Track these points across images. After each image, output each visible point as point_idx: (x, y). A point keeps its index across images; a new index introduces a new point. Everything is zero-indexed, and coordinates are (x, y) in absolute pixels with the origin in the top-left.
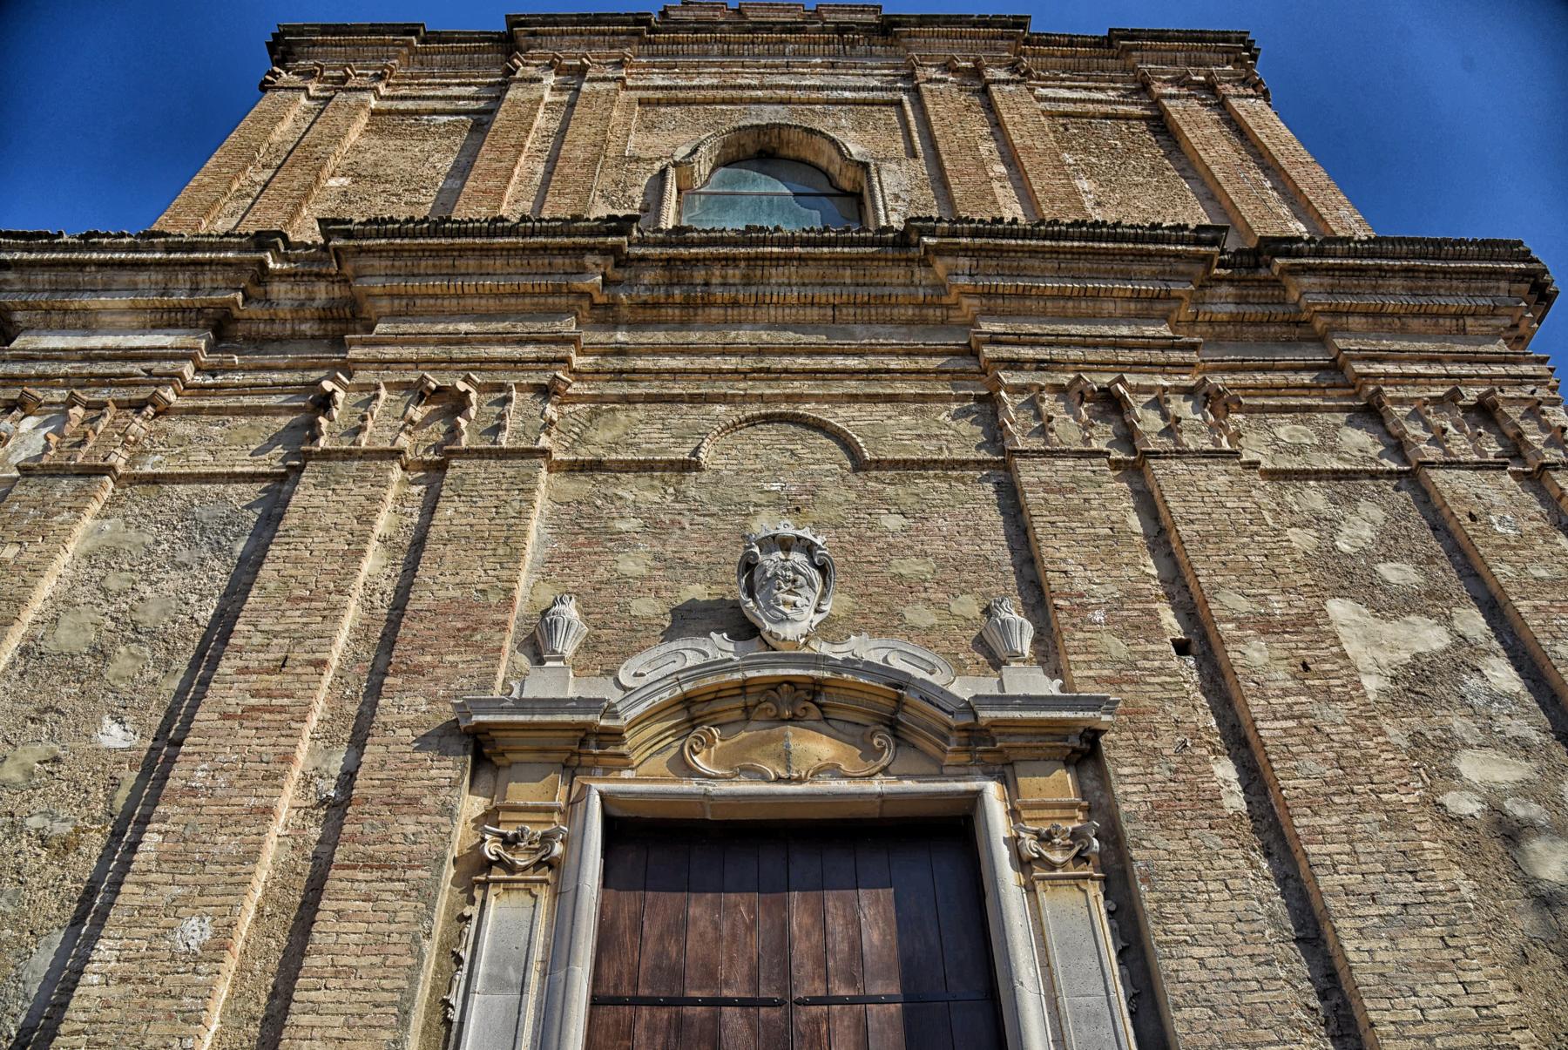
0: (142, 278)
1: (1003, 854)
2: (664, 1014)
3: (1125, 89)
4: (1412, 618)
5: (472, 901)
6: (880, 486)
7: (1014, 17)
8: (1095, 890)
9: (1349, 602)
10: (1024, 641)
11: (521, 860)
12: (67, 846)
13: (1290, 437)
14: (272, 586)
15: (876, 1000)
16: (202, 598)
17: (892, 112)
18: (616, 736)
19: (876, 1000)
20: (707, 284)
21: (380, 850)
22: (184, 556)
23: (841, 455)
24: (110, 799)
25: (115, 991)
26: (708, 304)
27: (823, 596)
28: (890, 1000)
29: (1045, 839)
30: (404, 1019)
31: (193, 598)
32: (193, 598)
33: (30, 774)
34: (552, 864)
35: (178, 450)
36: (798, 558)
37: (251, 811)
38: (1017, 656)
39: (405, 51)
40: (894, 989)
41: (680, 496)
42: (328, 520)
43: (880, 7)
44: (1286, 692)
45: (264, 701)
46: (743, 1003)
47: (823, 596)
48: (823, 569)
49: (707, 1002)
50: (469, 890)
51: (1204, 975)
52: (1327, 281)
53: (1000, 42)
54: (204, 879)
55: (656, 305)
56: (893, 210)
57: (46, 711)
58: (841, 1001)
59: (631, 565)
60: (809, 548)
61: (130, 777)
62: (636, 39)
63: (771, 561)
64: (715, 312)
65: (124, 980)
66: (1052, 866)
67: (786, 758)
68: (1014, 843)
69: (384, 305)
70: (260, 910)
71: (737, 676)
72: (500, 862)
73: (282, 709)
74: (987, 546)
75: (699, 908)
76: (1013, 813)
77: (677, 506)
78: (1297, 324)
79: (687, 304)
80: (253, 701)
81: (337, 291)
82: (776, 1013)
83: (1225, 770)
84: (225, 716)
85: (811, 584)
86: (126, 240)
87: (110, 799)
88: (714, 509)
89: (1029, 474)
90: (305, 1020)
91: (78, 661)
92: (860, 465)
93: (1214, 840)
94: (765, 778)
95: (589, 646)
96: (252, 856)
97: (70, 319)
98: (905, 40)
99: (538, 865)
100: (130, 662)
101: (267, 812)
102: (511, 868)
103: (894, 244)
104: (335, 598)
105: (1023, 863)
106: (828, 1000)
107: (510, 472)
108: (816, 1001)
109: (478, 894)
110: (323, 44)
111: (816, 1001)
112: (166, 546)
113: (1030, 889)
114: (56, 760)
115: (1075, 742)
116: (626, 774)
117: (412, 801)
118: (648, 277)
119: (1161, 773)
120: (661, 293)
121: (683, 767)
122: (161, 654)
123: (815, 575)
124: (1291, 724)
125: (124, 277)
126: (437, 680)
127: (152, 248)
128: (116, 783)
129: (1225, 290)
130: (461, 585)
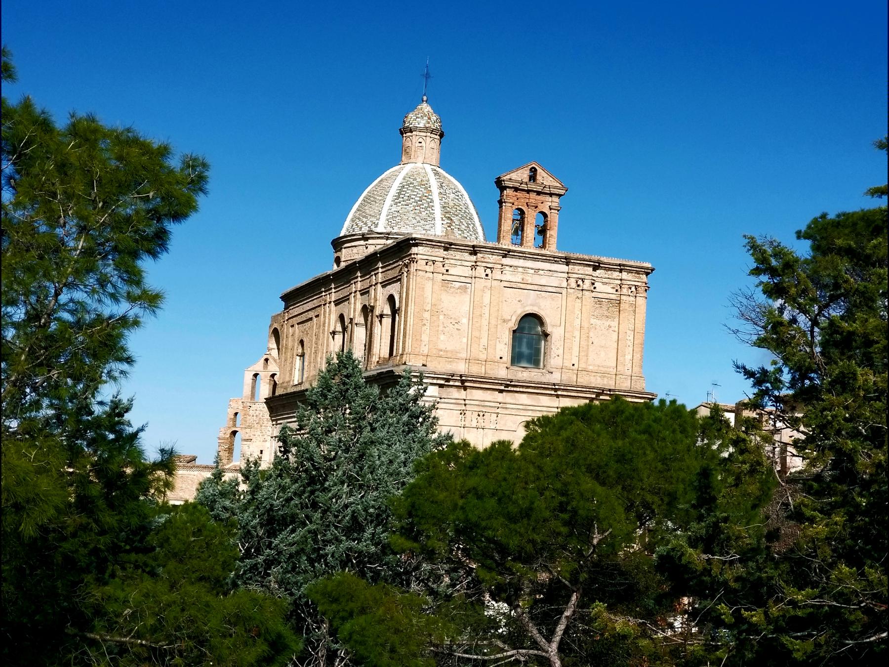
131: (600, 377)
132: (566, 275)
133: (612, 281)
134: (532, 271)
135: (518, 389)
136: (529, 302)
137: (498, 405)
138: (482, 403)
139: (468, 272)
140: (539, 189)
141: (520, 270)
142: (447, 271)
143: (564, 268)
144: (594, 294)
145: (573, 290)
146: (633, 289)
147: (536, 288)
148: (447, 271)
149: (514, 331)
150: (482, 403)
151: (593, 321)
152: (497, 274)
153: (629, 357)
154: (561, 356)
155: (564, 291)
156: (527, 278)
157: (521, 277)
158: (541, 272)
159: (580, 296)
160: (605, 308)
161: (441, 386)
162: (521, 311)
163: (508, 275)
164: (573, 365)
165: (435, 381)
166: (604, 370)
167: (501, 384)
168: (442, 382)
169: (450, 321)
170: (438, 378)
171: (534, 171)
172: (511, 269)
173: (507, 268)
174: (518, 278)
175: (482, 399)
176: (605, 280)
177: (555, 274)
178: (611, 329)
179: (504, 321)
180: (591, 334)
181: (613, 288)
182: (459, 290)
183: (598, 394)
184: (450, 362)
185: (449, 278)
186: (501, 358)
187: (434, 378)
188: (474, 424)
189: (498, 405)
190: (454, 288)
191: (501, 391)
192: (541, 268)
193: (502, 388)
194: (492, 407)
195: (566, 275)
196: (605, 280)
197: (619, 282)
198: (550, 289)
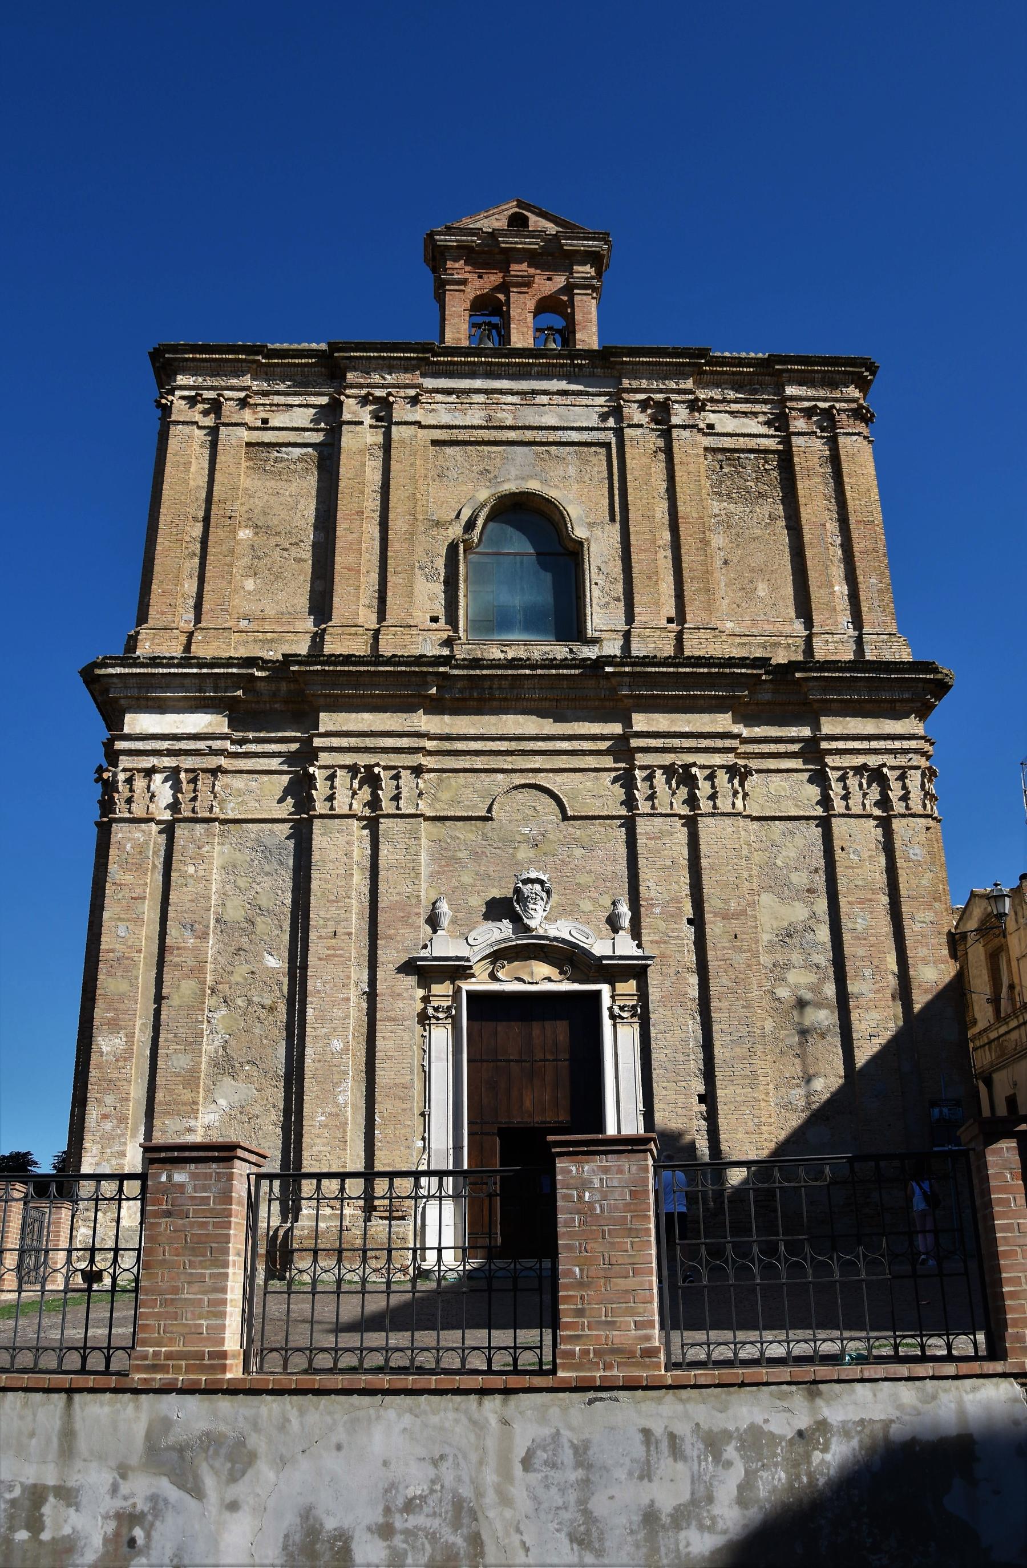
0: (187, 681)
1: (606, 1014)
2: (491, 1065)
3: (772, 414)
4: (796, 903)
5: (425, 1030)
6: (574, 830)
7: (699, 349)
8: (637, 1026)
9: (771, 895)
10: (626, 923)
11: (441, 1015)
12: (272, 1009)
13: (776, 791)
14: (319, 894)
15: (560, 1060)
16: (283, 892)
17: (603, 451)
18: (470, 968)
19: (560, 1060)
20: (491, 688)
21: (392, 1014)
22: (267, 868)
23: (557, 810)
24: (281, 990)
25: (317, 1065)
26: (492, 699)
27: (547, 903)
28: (565, 1060)
29: (622, 1008)
30: (412, 1072)
31: (280, 892)
32: (280, 892)
33: (246, 979)
34: (452, 1017)
35: (240, 799)
36: (538, 887)
37: (342, 999)
38: (621, 928)
39: (254, 366)
40: (567, 1057)
41: (485, 837)
42: (333, 856)
43: (608, 234)
44: (724, 948)
45: (333, 952)
46: (517, 1061)
47: (547, 903)
48: (548, 892)
49: (505, 1061)
50: (423, 1026)
51: (666, 1059)
52: (823, 683)
53: (687, 369)
54: (334, 1026)
55: (464, 699)
56: (596, 584)
57: (239, 949)
58: (549, 1060)
59: (467, 879)
60: (541, 882)
61: (286, 980)
62: (423, 363)
63: (527, 889)
64: (495, 704)
65: (319, 1061)
66: (623, 1018)
67: (532, 974)
68: (610, 1009)
69: (322, 701)
70: (353, 1034)
71: (514, 943)
72: (434, 1017)
73: (341, 956)
74: (618, 867)
75: (501, 1027)
76: (613, 997)
77: (484, 843)
78: (804, 704)
79: (480, 700)
80: (329, 952)
81: (292, 686)
82: (527, 1064)
83: (694, 980)
84: (320, 959)
85: (542, 899)
86: (176, 661)
87: (281, 990)
88: (500, 845)
89: (642, 826)
90: (381, 1073)
91: (242, 926)
92: (565, 818)
93: (680, 1011)
94: (524, 982)
95: (454, 921)
96: (347, 1017)
97: (150, 703)
98: (618, 367)
99: (446, 1018)
100: (264, 926)
101: (348, 999)
102: (438, 1019)
103: (589, 667)
104: (347, 900)
105: (613, 1017)
106: (545, 1060)
107: (409, 827)
108: (541, 1061)
109: (427, 1028)
110: (193, 359)
111: (541, 1061)
112: (256, 862)
113: (614, 1026)
114: (253, 972)
115: (638, 970)
116: (473, 980)
117: (399, 995)
118: (459, 685)
119: (668, 984)
120: (467, 695)
121: (493, 977)
122: (276, 922)
123: (544, 895)
124: (722, 963)
125: (177, 681)
126: (398, 942)
127: (191, 666)
128: (280, 983)
129: (768, 686)
130: (399, 894)
133: (757, 408)
136: (514, 472)
138: (370, 742)
140: (532, 244)
141: (481, 398)
145: (639, 431)
147: (529, 435)
148: (265, 421)
150: (370, 742)
151: (716, 506)
157: (483, 414)
169: (273, 541)
172: (453, 398)
173: (439, 397)
174: (476, 417)
176: (735, 407)
179: (437, 524)
182: (300, 466)
184: (272, 641)
185: (268, 437)
190: (282, 460)
196: (735, 407)
198: (575, 436)
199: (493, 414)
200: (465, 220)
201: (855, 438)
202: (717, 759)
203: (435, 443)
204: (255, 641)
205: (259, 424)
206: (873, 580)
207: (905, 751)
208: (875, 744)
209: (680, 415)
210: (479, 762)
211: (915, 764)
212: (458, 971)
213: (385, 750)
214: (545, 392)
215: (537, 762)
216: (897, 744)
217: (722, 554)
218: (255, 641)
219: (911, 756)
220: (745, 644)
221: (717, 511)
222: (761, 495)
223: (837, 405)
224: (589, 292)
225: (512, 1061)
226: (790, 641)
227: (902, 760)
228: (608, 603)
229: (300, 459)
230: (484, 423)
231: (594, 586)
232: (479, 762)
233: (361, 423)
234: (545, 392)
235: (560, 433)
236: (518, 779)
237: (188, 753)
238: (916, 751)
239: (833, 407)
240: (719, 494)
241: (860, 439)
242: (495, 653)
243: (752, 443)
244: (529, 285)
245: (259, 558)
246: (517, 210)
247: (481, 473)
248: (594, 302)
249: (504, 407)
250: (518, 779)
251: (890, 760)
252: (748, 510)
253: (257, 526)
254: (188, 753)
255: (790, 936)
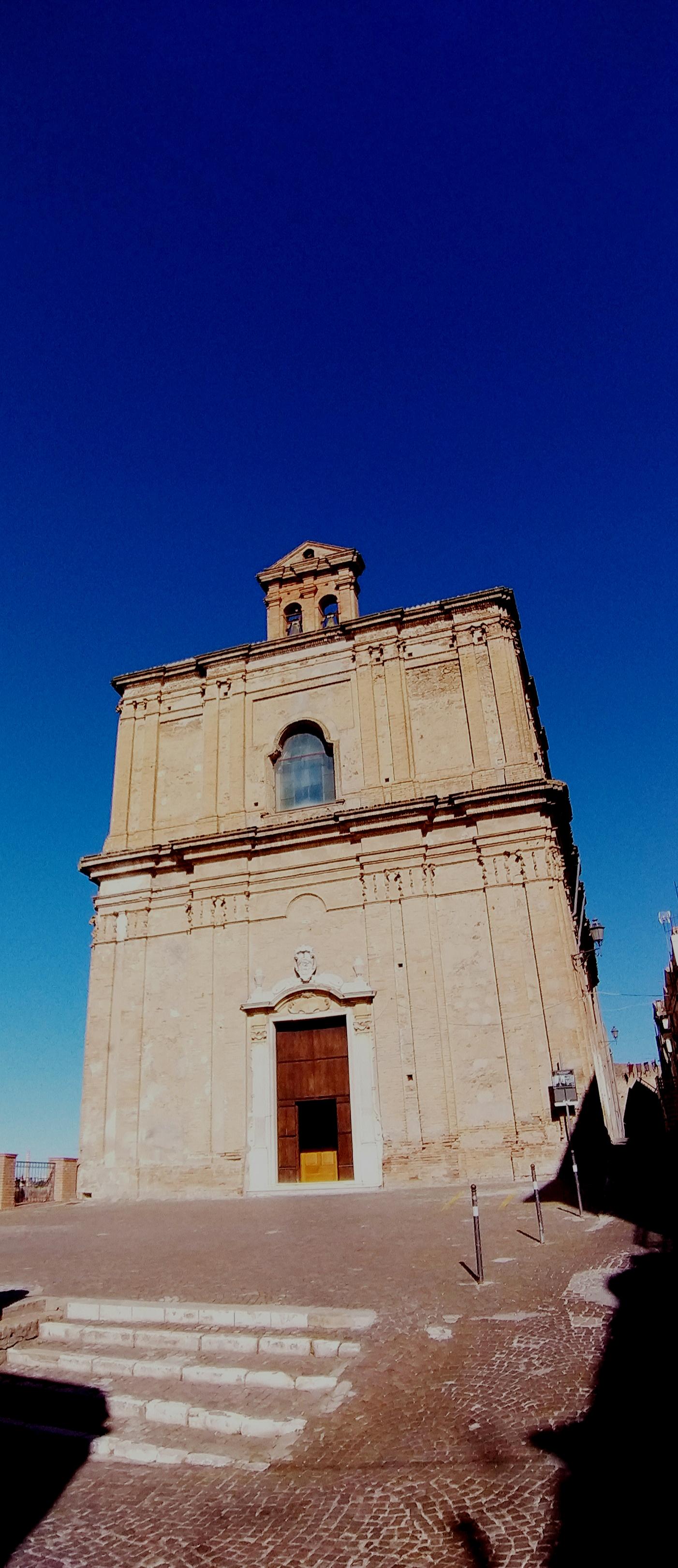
131: (443, 786)
132: (350, 653)
133: (438, 635)
134: (298, 665)
135: (279, 844)
137: (246, 878)
139: (198, 699)
142: (169, 708)
143: (344, 644)
144: (409, 664)
146: (478, 634)
148: (169, 708)
149: (274, 758)
151: (414, 703)
152: (238, 686)
153: (494, 739)
154: (361, 773)
155: (352, 675)
156: (289, 676)
157: (280, 678)
158: (311, 662)
159: (381, 673)
160: (435, 678)
161: (153, 872)
162: (281, 725)
163: (257, 682)
164: (387, 780)
165: (139, 866)
166: (447, 774)
167: (242, 842)
168: (151, 864)
170: (141, 860)
171: (309, 554)
174: (276, 681)
175: (216, 875)
176: (424, 639)
177: (336, 656)
178: (454, 705)
180: (415, 724)
181: (444, 644)
182: (188, 729)
183: (431, 812)
186: (256, 804)
187: (133, 861)
188: (207, 920)
189: (246, 878)
191: (250, 855)
192: (308, 656)
193: (248, 847)
194: (234, 884)
195: (350, 653)
196: (424, 639)
197: (450, 633)
199: (284, 677)
200: (279, 562)
201: (498, 640)
202: (413, 862)
203: (255, 701)
204: (165, 834)
205: (167, 710)
206: (512, 730)
207: (534, 838)
208: (512, 837)
209: (390, 651)
210: (280, 884)
211: (541, 846)
212: (268, 1010)
213: (227, 885)
214: (313, 657)
215: (311, 879)
216: (527, 835)
217: (419, 732)
218: (165, 834)
219: (537, 841)
220: (431, 787)
221: (416, 707)
222: (443, 690)
223: (486, 622)
224: (348, 586)
225: (302, 1061)
226: (460, 779)
227: (533, 844)
228: (351, 777)
229: (187, 726)
230: (280, 684)
231: (343, 769)
232: (280, 884)
233: (215, 699)
234: (313, 657)
235: (321, 679)
236: (300, 891)
237: (131, 902)
238: (540, 837)
239: (483, 624)
240: (417, 695)
241: (502, 640)
242: (295, 817)
243: (435, 659)
244: (315, 592)
245: (168, 786)
246: (308, 548)
247: (281, 713)
248: (352, 592)
249: (291, 671)
250: (293, 894)
251: (522, 846)
252: (434, 702)
253: (167, 768)
254: (131, 902)
255: (463, 968)
